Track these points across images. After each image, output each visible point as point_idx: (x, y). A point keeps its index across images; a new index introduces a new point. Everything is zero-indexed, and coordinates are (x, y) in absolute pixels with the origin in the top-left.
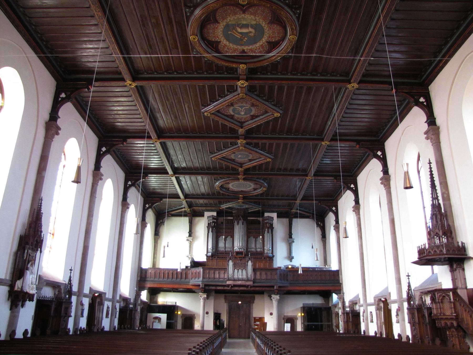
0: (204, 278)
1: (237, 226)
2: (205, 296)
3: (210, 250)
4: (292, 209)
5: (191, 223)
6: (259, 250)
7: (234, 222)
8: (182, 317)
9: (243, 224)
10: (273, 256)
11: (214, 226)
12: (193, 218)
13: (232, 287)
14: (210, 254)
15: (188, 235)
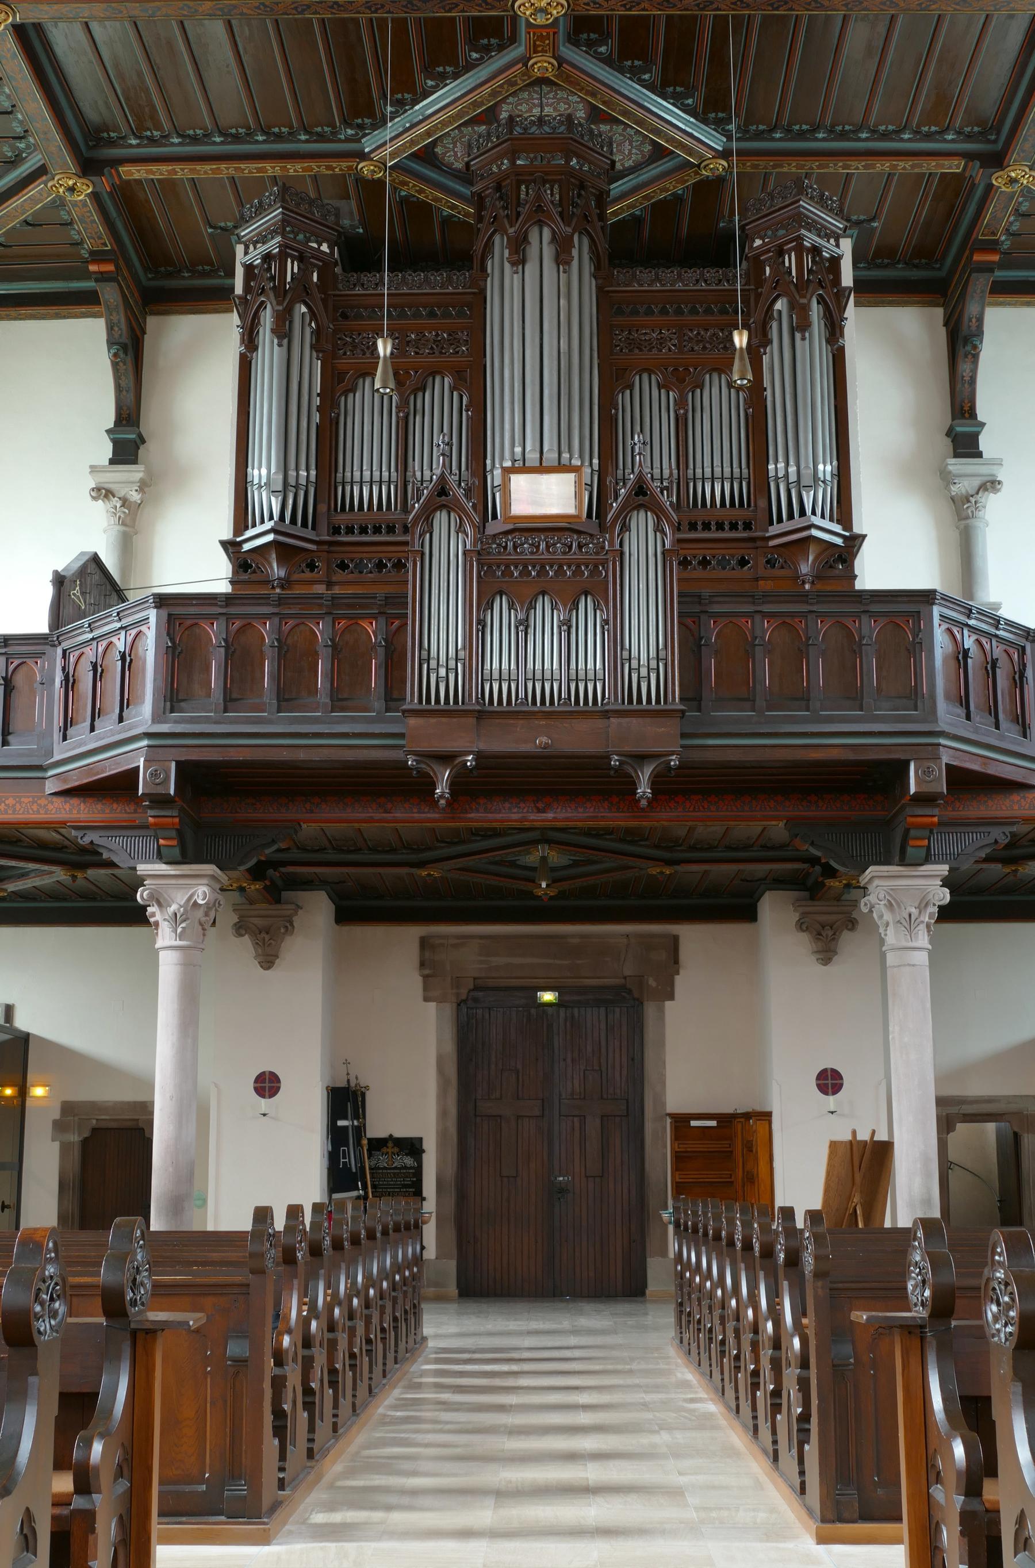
0: (174, 696)
1: (512, 280)
2: (202, 893)
3: (267, 502)
4: (997, 160)
5: (131, 355)
6: (716, 491)
7: (489, 246)
8: (59, 1127)
9: (562, 259)
10: (854, 542)
11: (302, 290)
12: (152, 322)
13: (461, 787)
14: (259, 536)
15: (106, 450)
